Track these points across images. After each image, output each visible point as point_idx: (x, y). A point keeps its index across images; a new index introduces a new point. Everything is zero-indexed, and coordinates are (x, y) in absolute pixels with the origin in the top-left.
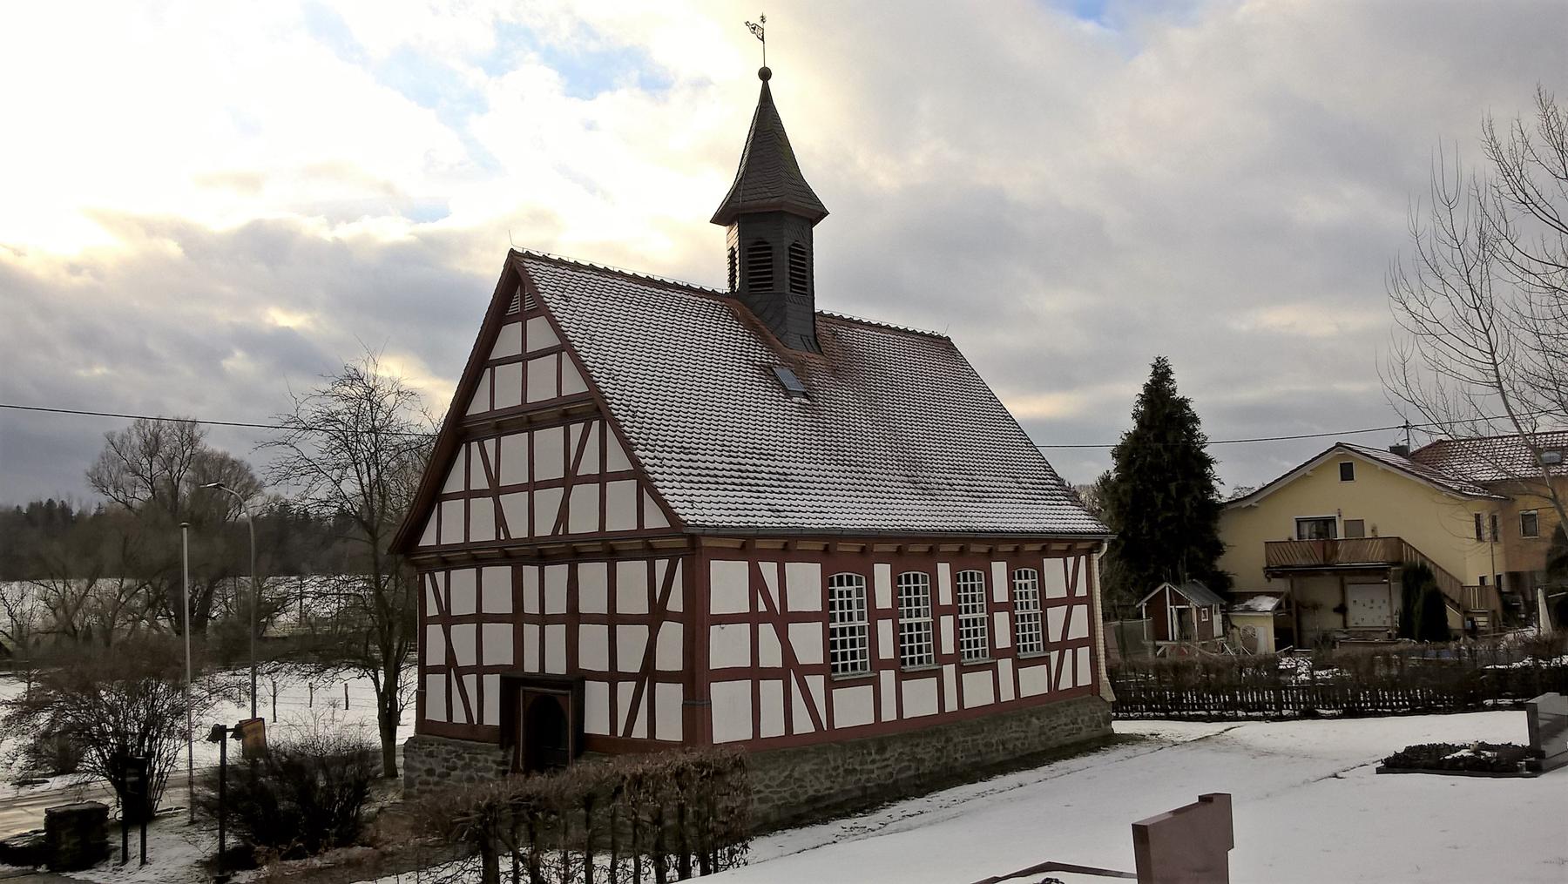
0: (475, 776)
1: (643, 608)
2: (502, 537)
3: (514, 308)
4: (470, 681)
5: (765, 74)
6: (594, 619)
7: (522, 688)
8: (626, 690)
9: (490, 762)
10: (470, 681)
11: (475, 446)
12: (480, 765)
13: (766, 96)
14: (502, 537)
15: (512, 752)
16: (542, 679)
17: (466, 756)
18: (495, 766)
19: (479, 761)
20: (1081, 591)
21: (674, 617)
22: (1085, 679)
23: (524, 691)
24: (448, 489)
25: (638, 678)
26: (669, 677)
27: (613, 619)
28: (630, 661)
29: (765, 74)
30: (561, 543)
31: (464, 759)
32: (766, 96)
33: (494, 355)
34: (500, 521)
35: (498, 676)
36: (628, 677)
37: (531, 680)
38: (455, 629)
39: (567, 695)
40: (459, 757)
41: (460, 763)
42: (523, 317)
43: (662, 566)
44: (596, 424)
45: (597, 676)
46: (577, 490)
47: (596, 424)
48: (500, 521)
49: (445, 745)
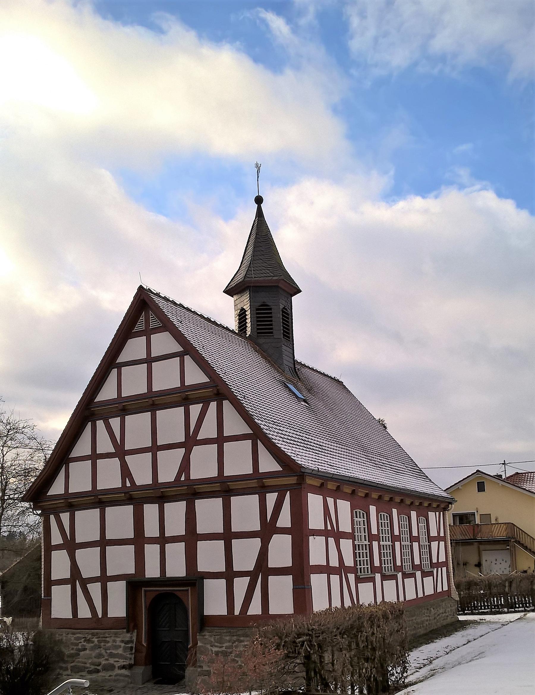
0: (104, 653)
2: (128, 484)
3: (140, 326)
4: (95, 589)
9: (118, 642)
10: (95, 589)
11: (100, 424)
12: (109, 644)
13: (260, 214)
14: (128, 484)
15: (135, 634)
17: (96, 640)
18: (123, 645)
19: (109, 642)
20: (442, 534)
22: (446, 588)
23: (145, 591)
24: (75, 454)
25: (253, 575)
30: (182, 486)
31: (93, 642)
32: (260, 214)
33: (121, 359)
34: (126, 472)
35: (124, 583)
37: (152, 582)
38: (79, 553)
39: (187, 590)
40: (89, 641)
41: (88, 646)
42: (148, 333)
44: (213, 405)
46: (197, 450)
47: (213, 405)
48: (126, 472)
49: (74, 634)
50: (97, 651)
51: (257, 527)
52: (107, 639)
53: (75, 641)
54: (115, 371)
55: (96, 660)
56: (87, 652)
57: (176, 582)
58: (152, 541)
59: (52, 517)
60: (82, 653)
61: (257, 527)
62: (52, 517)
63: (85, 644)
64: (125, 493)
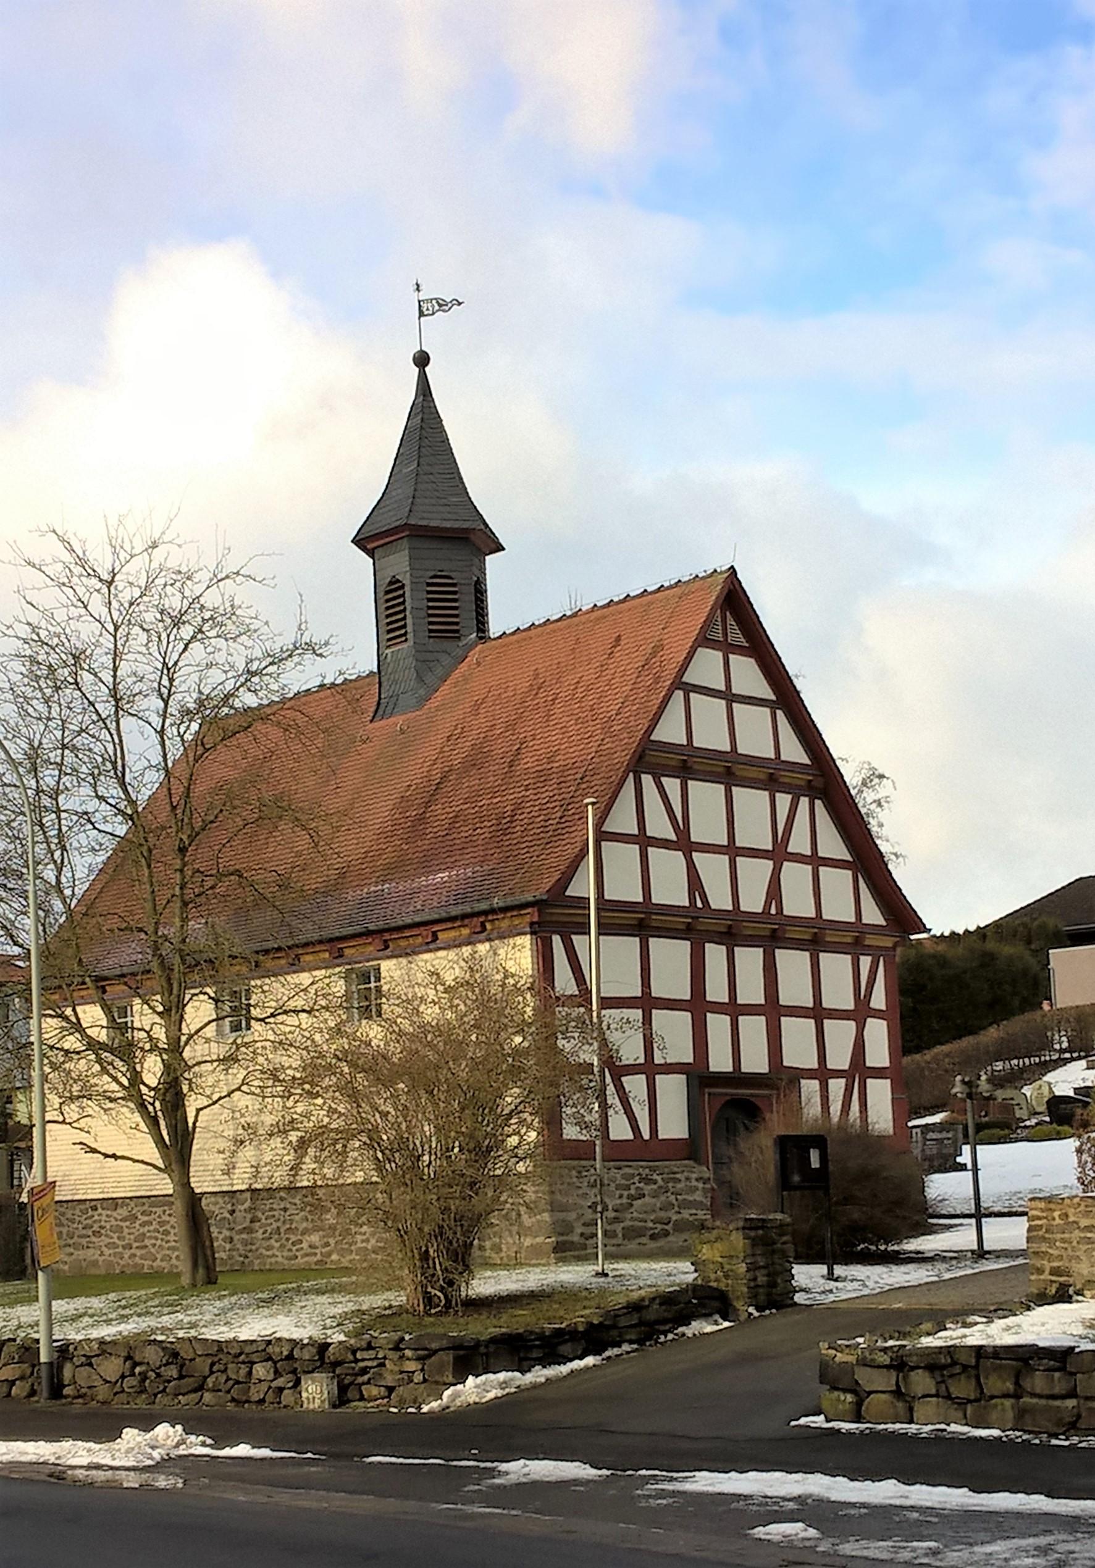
0: (674, 1201)
1: (848, 1003)
2: (699, 904)
4: (636, 1085)
5: (422, 360)
6: (751, 1010)
7: (707, 1090)
8: (837, 1086)
9: (683, 1179)
10: (636, 1085)
11: (647, 780)
13: (424, 388)
14: (699, 904)
16: (737, 1078)
17: (659, 1178)
18: (700, 1185)
21: (877, 1014)
23: (710, 1094)
26: (879, 1073)
27: (818, 1013)
28: (839, 1058)
29: (422, 360)
31: (655, 1182)
32: (424, 388)
36: (838, 1074)
37: (721, 1079)
40: (648, 1181)
41: (648, 1189)
43: (865, 962)
45: (810, 1074)
47: (804, 802)
49: (619, 1168)
50: (663, 1198)
51: (850, 1005)
52: (678, 1176)
53: (623, 1182)
54: (679, 694)
55: (662, 1214)
56: (647, 1199)
57: (754, 1080)
58: (718, 1008)
59: (557, 940)
60: (636, 1203)
61: (850, 1005)
62: (557, 940)
63: (642, 1185)
64: (692, 918)
